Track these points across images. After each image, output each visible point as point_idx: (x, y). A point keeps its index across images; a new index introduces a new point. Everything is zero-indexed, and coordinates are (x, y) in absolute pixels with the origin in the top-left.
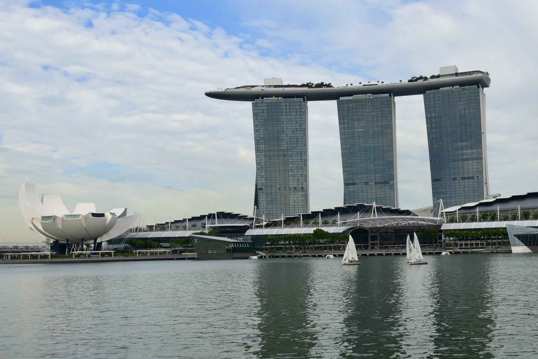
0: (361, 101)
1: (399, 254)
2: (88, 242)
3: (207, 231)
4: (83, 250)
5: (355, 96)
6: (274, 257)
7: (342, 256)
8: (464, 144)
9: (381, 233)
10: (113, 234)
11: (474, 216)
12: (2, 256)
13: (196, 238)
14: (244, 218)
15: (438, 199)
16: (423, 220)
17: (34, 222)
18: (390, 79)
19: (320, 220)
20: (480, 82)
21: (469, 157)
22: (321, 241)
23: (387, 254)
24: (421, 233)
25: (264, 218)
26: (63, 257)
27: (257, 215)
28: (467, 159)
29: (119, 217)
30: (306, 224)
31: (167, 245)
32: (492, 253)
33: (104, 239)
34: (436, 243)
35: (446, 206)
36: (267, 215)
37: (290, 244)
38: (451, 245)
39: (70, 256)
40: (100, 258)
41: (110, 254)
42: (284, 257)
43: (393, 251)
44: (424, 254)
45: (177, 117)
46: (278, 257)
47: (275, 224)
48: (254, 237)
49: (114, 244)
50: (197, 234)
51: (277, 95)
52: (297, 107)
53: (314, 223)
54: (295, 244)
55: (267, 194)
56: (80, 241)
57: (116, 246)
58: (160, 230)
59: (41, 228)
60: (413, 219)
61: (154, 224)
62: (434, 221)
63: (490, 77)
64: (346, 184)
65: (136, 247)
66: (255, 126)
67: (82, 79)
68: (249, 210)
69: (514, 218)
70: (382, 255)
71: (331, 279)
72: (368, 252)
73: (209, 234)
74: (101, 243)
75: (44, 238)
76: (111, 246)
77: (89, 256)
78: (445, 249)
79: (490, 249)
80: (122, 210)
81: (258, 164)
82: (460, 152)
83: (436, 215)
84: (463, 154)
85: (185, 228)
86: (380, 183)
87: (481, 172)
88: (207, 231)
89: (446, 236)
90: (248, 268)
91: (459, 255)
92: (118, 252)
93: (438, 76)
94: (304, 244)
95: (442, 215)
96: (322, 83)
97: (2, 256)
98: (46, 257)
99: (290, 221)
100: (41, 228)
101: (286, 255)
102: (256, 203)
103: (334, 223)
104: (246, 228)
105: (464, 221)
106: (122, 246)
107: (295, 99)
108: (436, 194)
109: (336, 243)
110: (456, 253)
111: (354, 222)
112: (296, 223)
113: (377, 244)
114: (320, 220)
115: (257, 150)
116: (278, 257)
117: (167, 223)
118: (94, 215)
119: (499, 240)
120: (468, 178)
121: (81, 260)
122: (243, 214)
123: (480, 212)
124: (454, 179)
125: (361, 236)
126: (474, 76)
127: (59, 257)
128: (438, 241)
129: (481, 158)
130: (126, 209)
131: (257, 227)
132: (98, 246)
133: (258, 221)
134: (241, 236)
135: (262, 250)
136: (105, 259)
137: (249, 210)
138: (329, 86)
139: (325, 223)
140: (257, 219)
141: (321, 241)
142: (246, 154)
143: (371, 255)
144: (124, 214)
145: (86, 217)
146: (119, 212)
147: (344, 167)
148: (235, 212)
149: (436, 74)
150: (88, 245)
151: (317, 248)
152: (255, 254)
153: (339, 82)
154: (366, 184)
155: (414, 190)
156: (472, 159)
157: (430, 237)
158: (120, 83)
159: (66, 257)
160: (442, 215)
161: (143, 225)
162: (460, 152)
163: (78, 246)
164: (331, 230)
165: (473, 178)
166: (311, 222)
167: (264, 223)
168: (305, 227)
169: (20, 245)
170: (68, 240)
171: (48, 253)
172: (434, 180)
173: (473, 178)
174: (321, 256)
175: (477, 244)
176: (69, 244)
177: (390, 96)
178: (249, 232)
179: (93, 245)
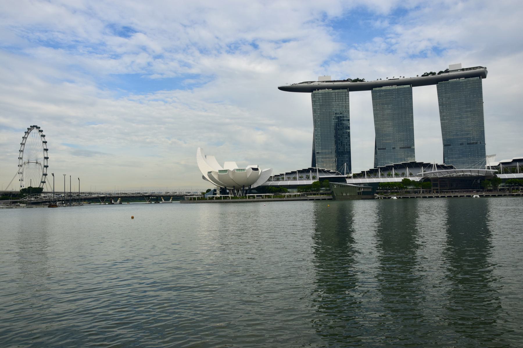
19: (393, 172)
20: (483, 75)
63: (487, 69)
165: (477, 143)
166: (386, 174)
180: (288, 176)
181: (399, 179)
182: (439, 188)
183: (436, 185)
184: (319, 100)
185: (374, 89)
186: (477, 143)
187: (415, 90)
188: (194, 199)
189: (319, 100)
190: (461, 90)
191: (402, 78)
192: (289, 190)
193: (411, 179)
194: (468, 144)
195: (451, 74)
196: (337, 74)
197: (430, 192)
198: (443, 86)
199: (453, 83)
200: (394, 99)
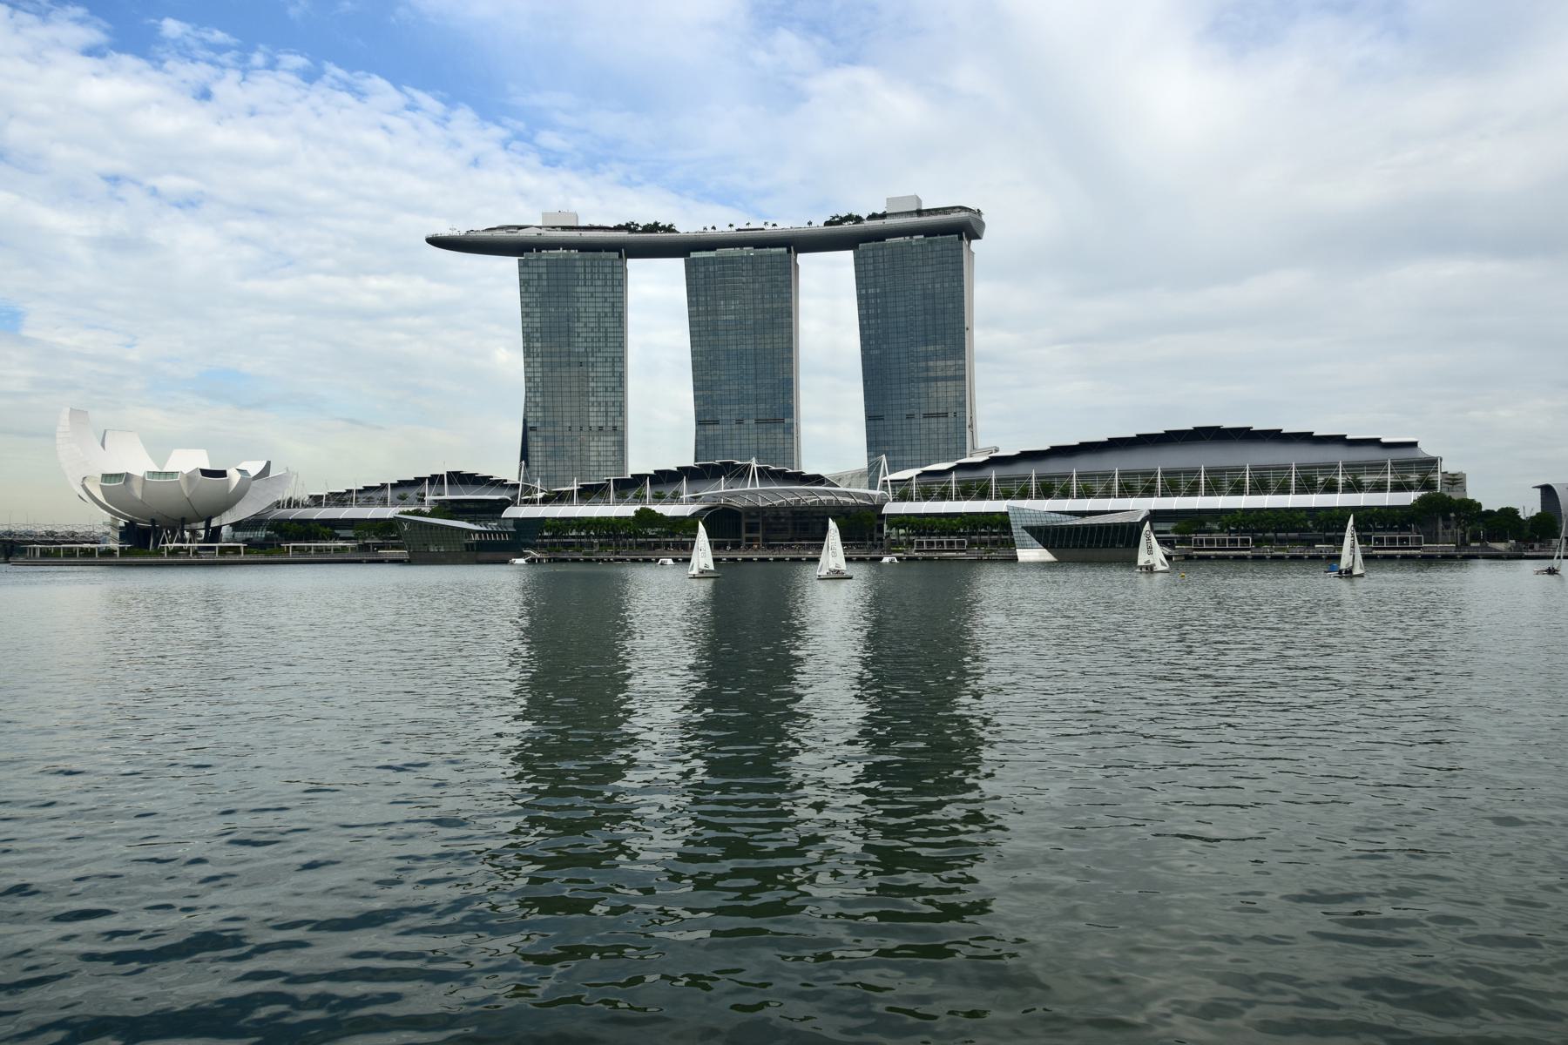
0: (732, 260)
1: (799, 560)
2: (194, 525)
3: (427, 509)
4: (184, 541)
5: (720, 251)
6: (556, 560)
7: (688, 560)
8: (931, 348)
9: (765, 519)
10: (243, 511)
11: (946, 489)
12: (25, 550)
13: (406, 521)
14: (501, 484)
15: (878, 454)
16: (848, 494)
17: (88, 485)
18: (789, 221)
19: (648, 491)
21: (940, 374)
22: (650, 531)
23: (776, 560)
24: (843, 519)
25: (538, 485)
26: (144, 555)
27: (526, 479)
28: (936, 379)
29: (256, 478)
30: (621, 498)
31: (350, 533)
32: (980, 560)
33: (225, 521)
34: (871, 539)
35: (893, 468)
36: (546, 479)
37: (588, 536)
38: (901, 544)
39: (159, 553)
40: (218, 558)
41: (236, 550)
42: (577, 560)
43: (788, 555)
44: (848, 560)
45: (373, 282)
46: (565, 560)
47: (562, 498)
48: (518, 522)
49: (244, 530)
50: (408, 513)
51: (568, 245)
52: (607, 270)
53: (636, 497)
54: (598, 536)
55: (545, 439)
56: (177, 524)
57: (249, 535)
58: (336, 505)
59: (101, 498)
60: (829, 493)
61: (324, 493)
62: (869, 497)
64: (701, 422)
65: (286, 537)
66: (524, 305)
67: (188, 204)
68: (509, 469)
69: (1024, 495)
70: (766, 560)
71: (665, 604)
72: (740, 556)
73: (432, 514)
74: (220, 528)
75: (107, 517)
76: (238, 535)
77: (195, 553)
78: (889, 553)
79: (976, 552)
80: (261, 465)
81: (528, 379)
82: (923, 364)
83: (872, 486)
84: (927, 369)
85: (384, 502)
86: (766, 421)
87: (963, 404)
88: (427, 509)
89: (890, 527)
90: (504, 586)
91: (915, 565)
92: (252, 546)
93: (884, 216)
94: (616, 536)
95: (884, 486)
96: (656, 224)
97: (25, 550)
98: (110, 553)
99: (589, 493)
100: (101, 498)
101: (581, 557)
102: (525, 455)
103: (676, 498)
104: (504, 504)
105: (926, 498)
106: (261, 534)
107: (604, 254)
108: (875, 444)
109: (676, 537)
110: (909, 559)
111: (714, 496)
112: (601, 495)
113: (757, 539)
114: (648, 491)
115: (528, 352)
116: (565, 560)
117: (349, 491)
118: (205, 473)
119: (994, 537)
120: (938, 415)
121: (180, 560)
122: (498, 475)
123: (958, 482)
124: (910, 417)
125: (725, 524)
126: (953, 216)
127: (137, 555)
128: (876, 535)
129: (963, 378)
130: (269, 463)
131: (526, 502)
132: (214, 535)
133: (528, 490)
134: (493, 520)
135: (534, 547)
136: (226, 559)
137: (509, 469)
138: (669, 229)
139: (659, 498)
140: (526, 488)
141: (650, 531)
142: (508, 359)
143: (745, 560)
144: (265, 472)
145: (190, 478)
146: (254, 468)
147: (696, 389)
148: (483, 472)
149: (880, 212)
150: (194, 532)
151: (640, 545)
152: (522, 555)
153: (688, 226)
154: (740, 422)
155: (831, 434)
156: (946, 379)
157: (864, 528)
158: (262, 212)
159: (150, 555)
160: (884, 486)
161: (303, 495)
162: (923, 364)
163: (173, 533)
164: (669, 510)
166: (631, 495)
167: (540, 495)
168: (618, 503)
169: (60, 530)
170: (153, 522)
171: (115, 546)
172: (870, 418)
173: (946, 415)
174: (649, 561)
175: (951, 544)
176: (156, 530)
177: (789, 251)
178: (511, 512)
179: (203, 532)
180: (401, 492)
181: (629, 510)
182: (760, 535)
183: (752, 528)
184: (540, 278)
185: (693, 255)
186: (946, 415)
187: (807, 262)
188: (70, 553)
189: (540, 278)
190: (917, 268)
191: (769, 227)
192: (343, 533)
193: (659, 509)
194: (927, 416)
195: (888, 221)
196: (603, 206)
197: (736, 546)
198: (938, 248)
199: (893, 246)
200: (741, 283)
